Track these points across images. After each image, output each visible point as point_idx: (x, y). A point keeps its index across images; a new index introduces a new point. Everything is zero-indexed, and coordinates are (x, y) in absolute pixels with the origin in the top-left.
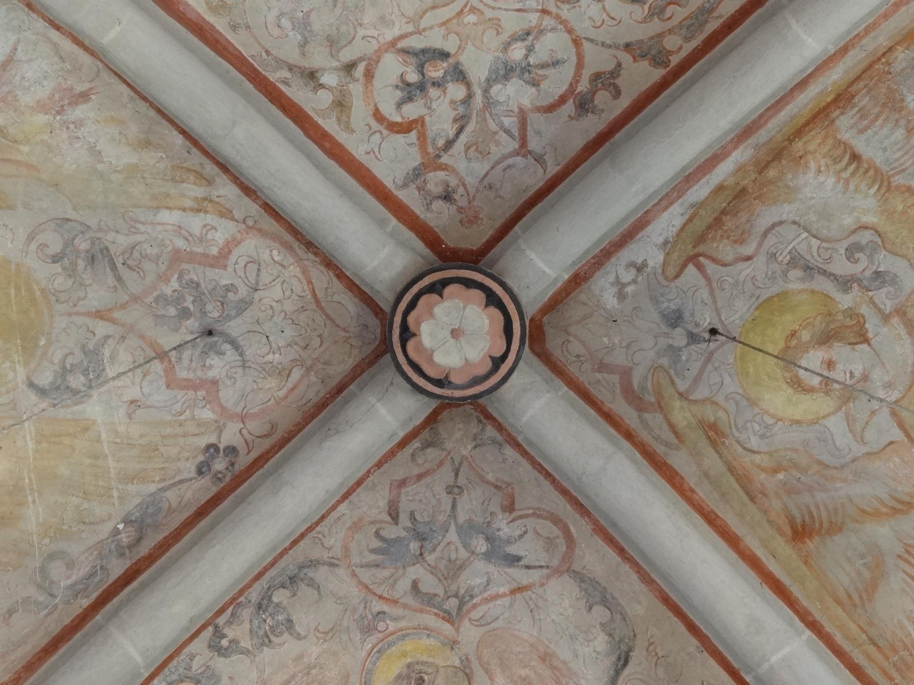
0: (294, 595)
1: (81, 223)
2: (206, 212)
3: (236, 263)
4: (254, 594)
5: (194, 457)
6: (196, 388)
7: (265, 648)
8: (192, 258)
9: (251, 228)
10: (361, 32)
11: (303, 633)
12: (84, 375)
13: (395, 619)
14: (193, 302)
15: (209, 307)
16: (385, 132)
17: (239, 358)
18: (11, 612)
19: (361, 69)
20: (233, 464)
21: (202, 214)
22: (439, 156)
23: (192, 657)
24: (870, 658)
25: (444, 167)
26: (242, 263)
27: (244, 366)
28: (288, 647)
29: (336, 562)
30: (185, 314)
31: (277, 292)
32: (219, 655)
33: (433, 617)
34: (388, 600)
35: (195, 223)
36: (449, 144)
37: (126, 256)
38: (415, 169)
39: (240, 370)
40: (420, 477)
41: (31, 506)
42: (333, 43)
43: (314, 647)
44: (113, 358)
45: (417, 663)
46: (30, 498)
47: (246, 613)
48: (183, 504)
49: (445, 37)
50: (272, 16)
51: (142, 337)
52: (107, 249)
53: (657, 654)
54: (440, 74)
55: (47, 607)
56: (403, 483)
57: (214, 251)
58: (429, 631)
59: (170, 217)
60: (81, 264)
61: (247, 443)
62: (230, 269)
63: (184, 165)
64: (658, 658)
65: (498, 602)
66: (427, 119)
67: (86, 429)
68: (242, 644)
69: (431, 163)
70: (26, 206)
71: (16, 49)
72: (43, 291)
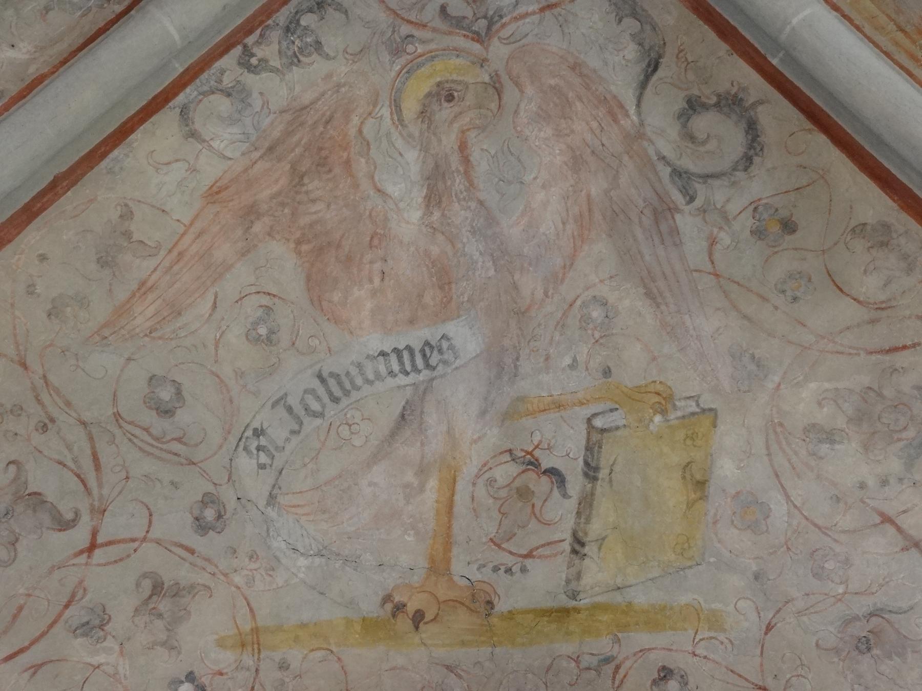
7: (294, 68)
11: (332, 54)
13: (423, 42)
23: (223, 72)
24: (897, 44)
28: (317, 66)
33: (462, 38)
34: (416, 24)
43: (343, 68)
45: (447, 82)
47: (275, 35)
53: (686, 59)
55: (81, 8)
58: (458, 52)
64: (688, 63)
65: (527, 20)
68: (272, 63)
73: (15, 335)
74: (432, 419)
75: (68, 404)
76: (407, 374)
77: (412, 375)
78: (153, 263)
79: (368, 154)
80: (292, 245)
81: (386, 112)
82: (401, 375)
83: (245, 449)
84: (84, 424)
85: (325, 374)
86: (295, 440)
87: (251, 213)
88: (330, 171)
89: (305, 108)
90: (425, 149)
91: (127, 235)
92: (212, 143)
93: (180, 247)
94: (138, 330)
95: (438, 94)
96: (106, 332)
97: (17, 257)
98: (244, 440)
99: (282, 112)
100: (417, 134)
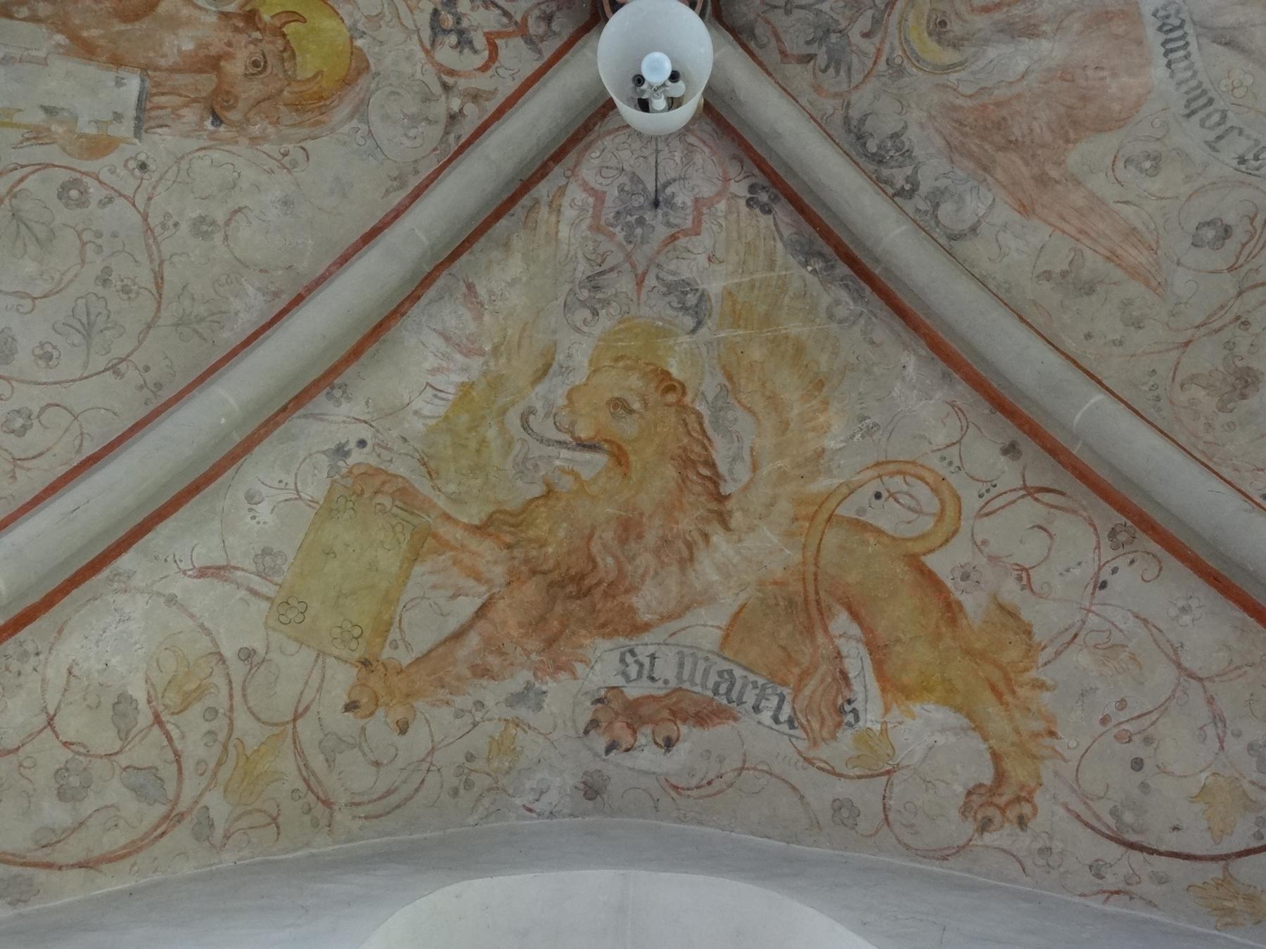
0: (872, 135)
1: (568, 295)
2: (560, 206)
3: (601, 184)
4: (871, 167)
5: (757, 216)
6: (701, 214)
8: (596, 217)
9: (573, 172)
10: (419, 75)
11: (902, 124)
12: (687, 294)
13: (893, 49)
14: (631, 215)
15: (636, 204)
16: (497, 64)
17: (677, 182)
18: (872, 342)
19: (446, 79)
20: (764, 188)
21: (562, 209)
22: (516, 23)
23: (918, 210)
25: (525, 19)
26: (602, 180)
27: (685, 179)
28: (913, 136)
29: (846, 103)
30: (641, 221)
31: (625, 154)
32: (917, 190)
33: (890, 18)
34: (877, 57)
35: (569, 213)
36: (506, 13)
37: (594, 264)
38: (526, 42)
39: (686, 182)
40: (779, 39)
41: (789, 331)
42: (427, 98)
43: (914, 115)
44: (674, 273)
45: (928, 27)
46: (783, 332)
47: (885, 172)
48: (794, 224)
49: (422, 11)
50: (407, 143)
51: (658, 252)
52: (588, 278)
54: (450, 17)
55: (870, 318)
56: (783, 53)
57: (591, 200)
58: (903, 19)
59: (564, 231)
60: (600, 295)
61: (747, 177)
62: (606, 189)
63: (523, 219)
66: (486, 30)
67: (730, 293)
69: (521, 29)
70: (554, 332)
71: (434, 329)
72: (620, 322)
73: (1160, 352)
74: (1228, 19)
75: (1222, 307)
76: (1187, 44)
77: (1189, 39)
78: (1088, 253)
79: (990, 89)
80: (1071, 146)
81: (953, 77)
82: (1190, 48)
83: (1258, 169)
84: (1240, 294)
85: (1187, 111)
86: (1247, 131)
87: (1042, 181)
88: (1004, 119)
89: (948, 143)
90: (986, 42)
91: (1064, 274)
92: (980, 215)
93: (1074, 232)
94: (1151, 260)
95: (939, 34)
96: (1154, 284)
97: (1088, 355)
98: (1250, 171)
99: (952, 162)
100: (973, 49)
